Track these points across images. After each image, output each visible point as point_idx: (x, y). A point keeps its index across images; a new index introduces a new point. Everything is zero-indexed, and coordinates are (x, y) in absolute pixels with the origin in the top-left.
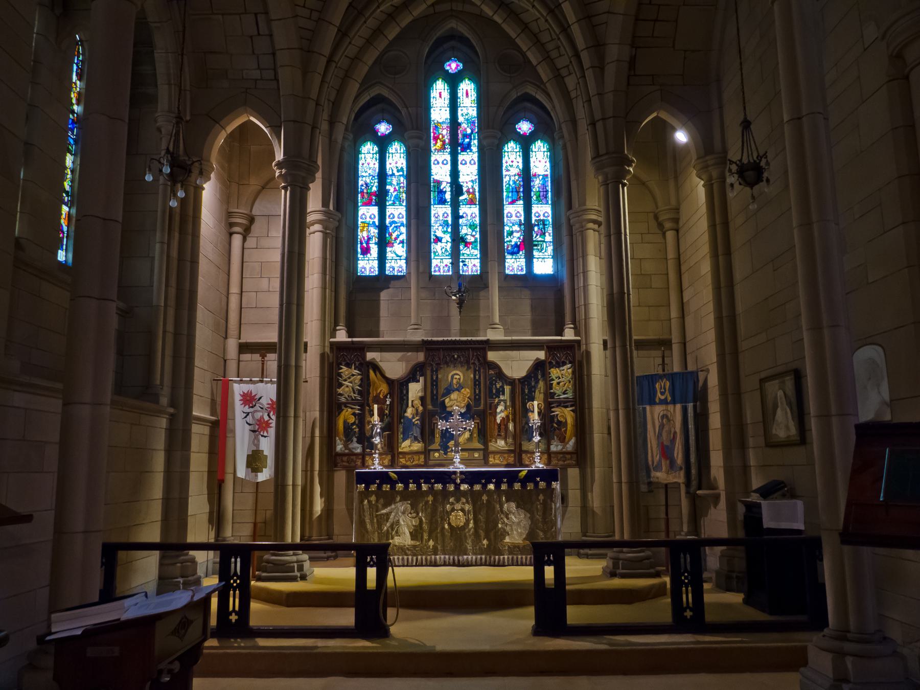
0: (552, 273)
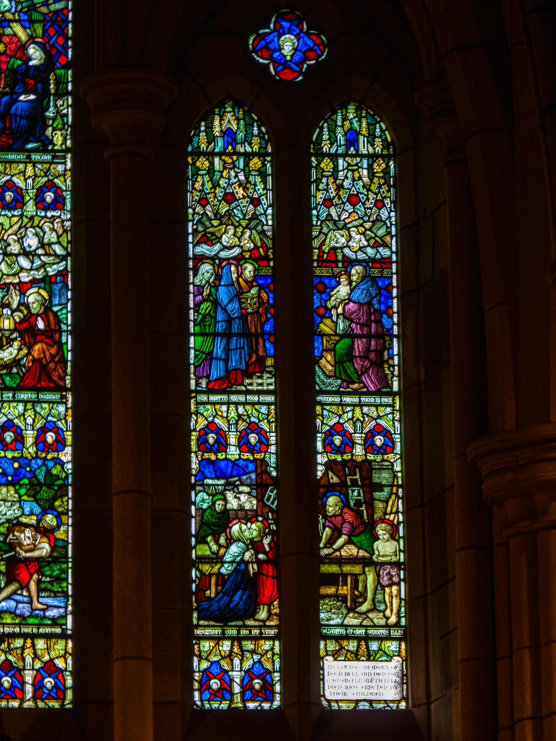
0: (403, 705)
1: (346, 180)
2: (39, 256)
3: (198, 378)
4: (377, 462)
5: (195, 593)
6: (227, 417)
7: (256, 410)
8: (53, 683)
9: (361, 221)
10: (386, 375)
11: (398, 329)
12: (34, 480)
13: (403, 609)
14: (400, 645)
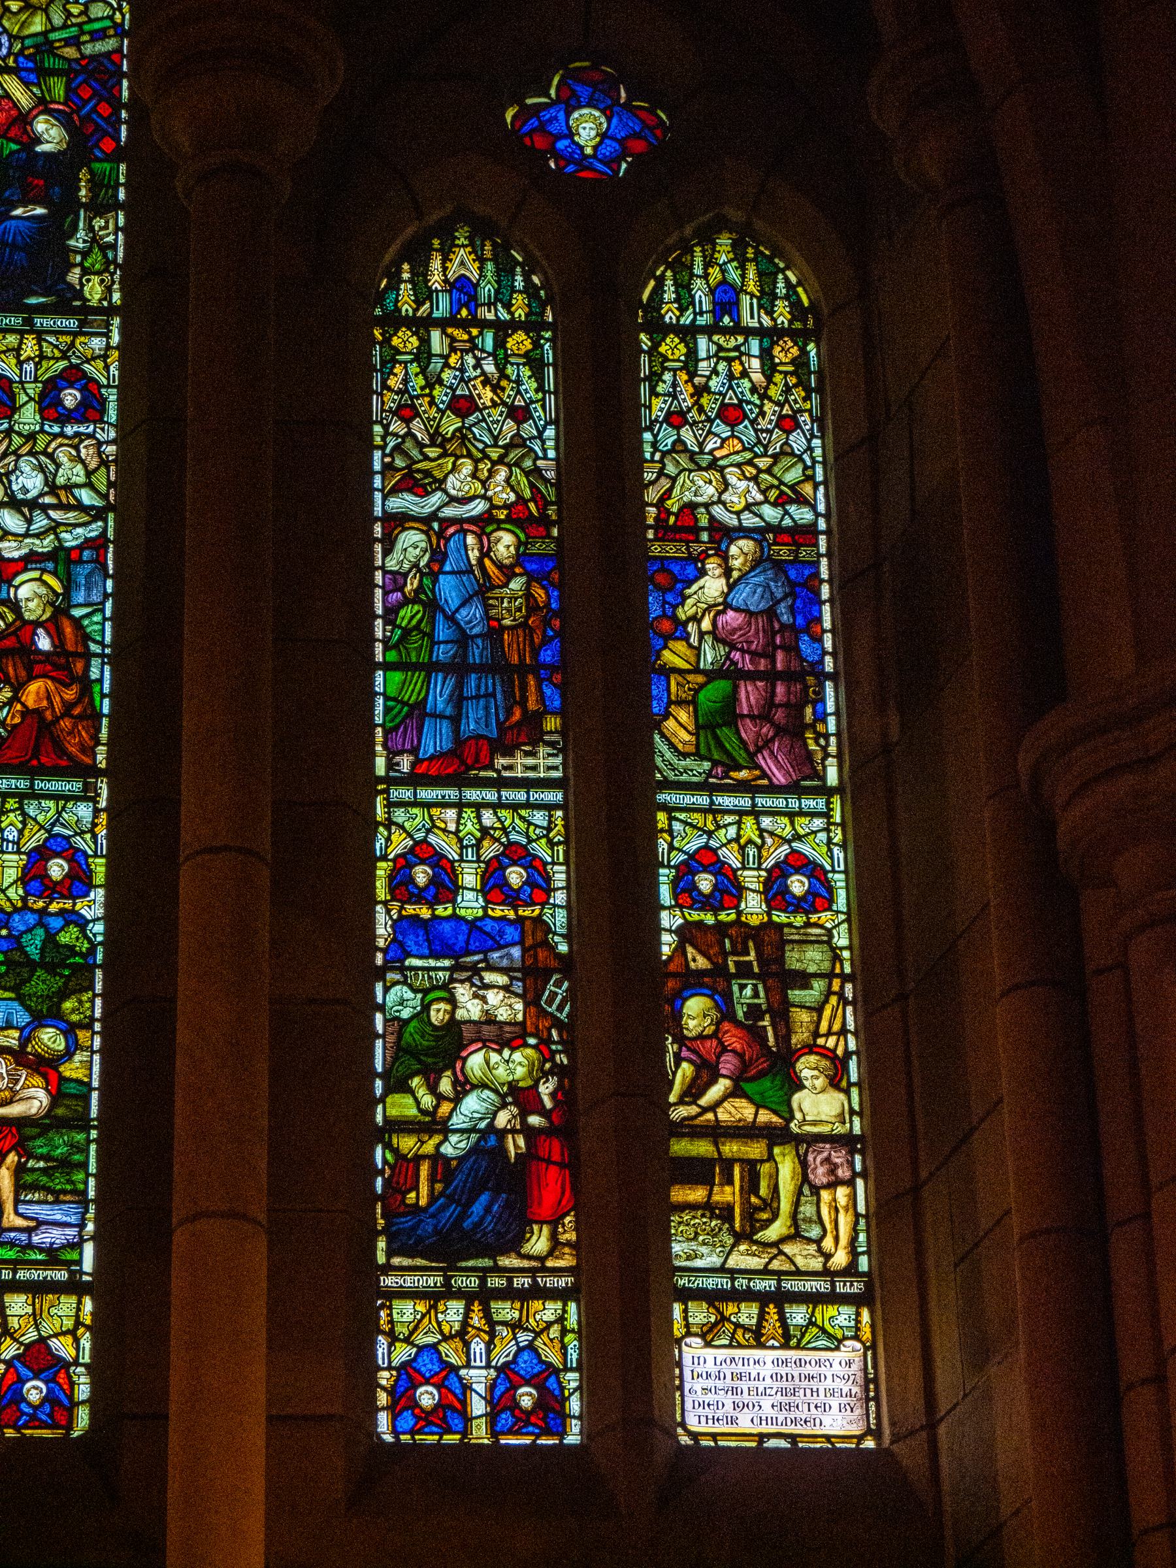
0: (870, 1444)
1: (714, 377)
2: (45, 508)
3: (392, 754)
4: (796, 928)
5: (381, 1198)
6: (458, 831)
7: (521, 818)
8: (45, 1391)
9: (748, 455)
10: (810, 755)
11: (835, 663)
12: (16, 956)
13: (862, 1237)
14: (858, 1314)
